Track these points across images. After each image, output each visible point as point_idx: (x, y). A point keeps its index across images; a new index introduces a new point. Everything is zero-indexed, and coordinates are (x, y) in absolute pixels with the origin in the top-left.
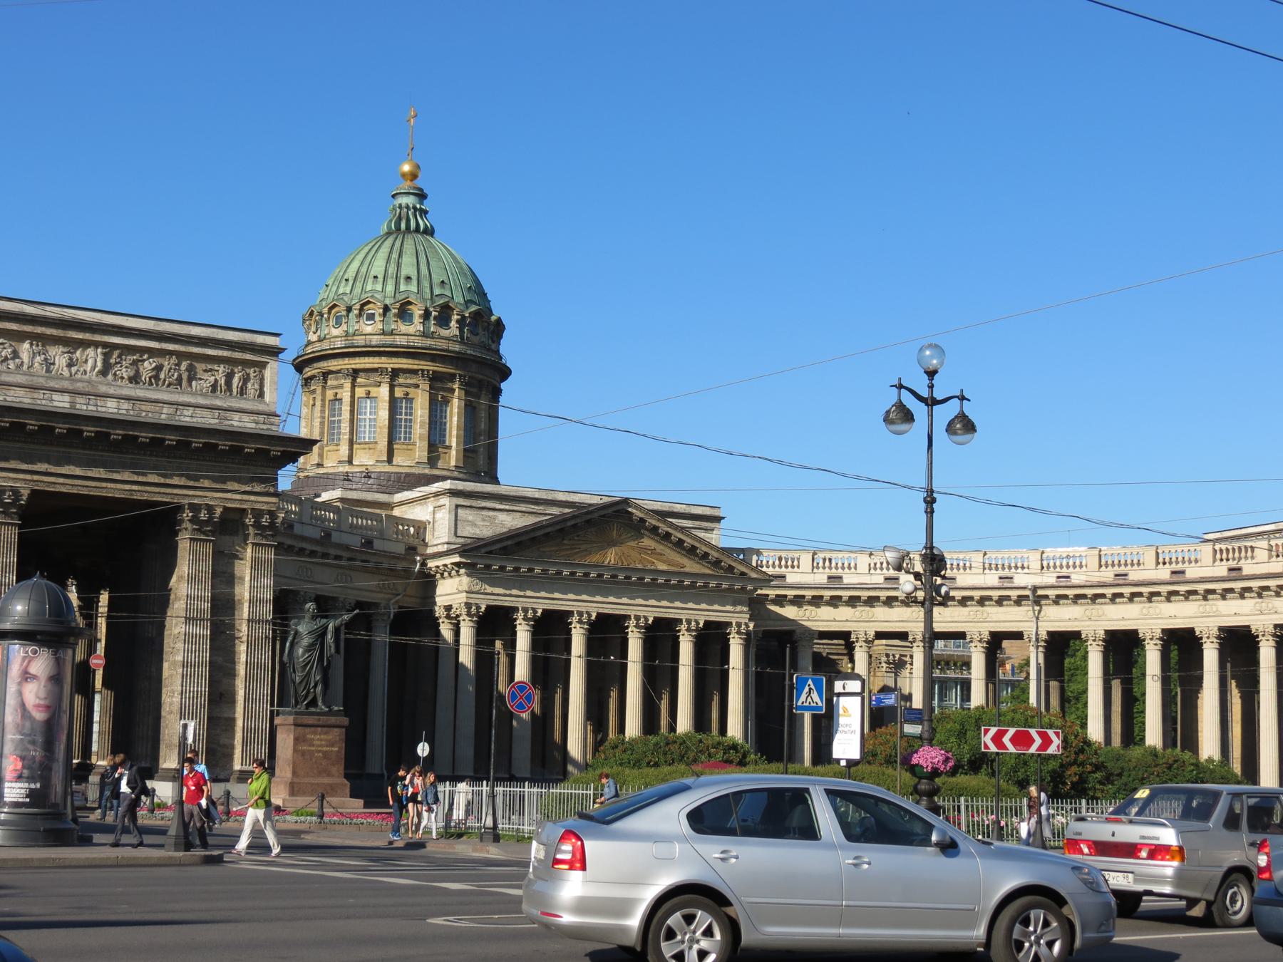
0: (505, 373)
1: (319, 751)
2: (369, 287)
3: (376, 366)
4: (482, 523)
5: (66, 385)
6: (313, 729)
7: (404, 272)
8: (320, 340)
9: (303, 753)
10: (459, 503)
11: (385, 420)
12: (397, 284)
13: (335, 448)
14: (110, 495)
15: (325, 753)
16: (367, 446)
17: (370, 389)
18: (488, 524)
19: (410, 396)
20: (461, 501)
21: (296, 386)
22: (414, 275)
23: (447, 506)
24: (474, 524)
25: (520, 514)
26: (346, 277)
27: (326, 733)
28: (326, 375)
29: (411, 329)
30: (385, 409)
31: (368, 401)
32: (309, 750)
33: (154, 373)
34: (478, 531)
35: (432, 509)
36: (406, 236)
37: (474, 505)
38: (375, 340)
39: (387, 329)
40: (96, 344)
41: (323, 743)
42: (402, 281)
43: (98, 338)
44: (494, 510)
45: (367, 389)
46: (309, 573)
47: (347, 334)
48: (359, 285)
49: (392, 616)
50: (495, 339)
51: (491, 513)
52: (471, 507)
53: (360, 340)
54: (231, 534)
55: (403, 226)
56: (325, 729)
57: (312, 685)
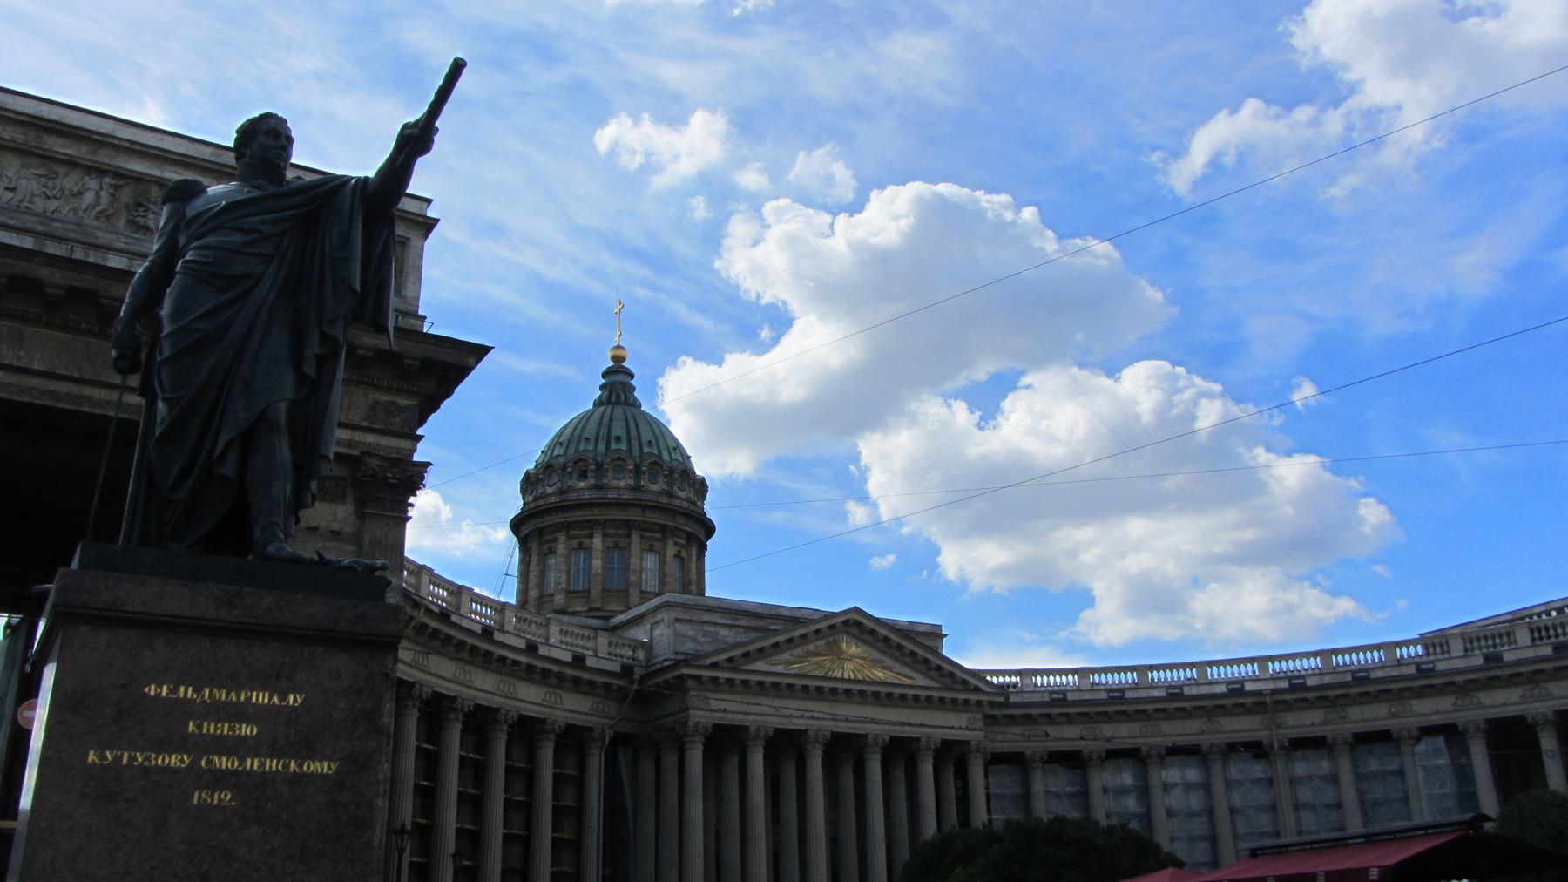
0: (709, 529)
1: (220, 779)
2: (582, 448)
3: (589, 518)
4: (703, 639)
5: (32, 222)
7: (615, 433)
8: (536, 499)
10: (677, 617)
11: (598, 568)
14: (97, 411)
16: (580, 595)
18: (710, 640)
19: (622, 545)
22: (624, 436)
23: (666, 621)
24: (694, 640)
25: (742, 630)
26: (560, 440)
28: (541, 531)
29: (622, 484)
32: (146, 771)
34: (699, 648)
35: (648, 627)
36: (615, 409)
37: (695, 618)
38: (587, 495)
40: (99, 171)
41: (246, 730)
42: (612, 441)
43: (105, 158)
44: (716, 624)
45: (580, 540)
46: (512, 690)
47: (561, 492)
48: (572, 447)
49: (607, 743)
50: (700, 496)
51: (712, 629)
52: (690, 621)
53: (573, 496)
54: (332, 501)
55: (613, 399)
57: (224, 438)
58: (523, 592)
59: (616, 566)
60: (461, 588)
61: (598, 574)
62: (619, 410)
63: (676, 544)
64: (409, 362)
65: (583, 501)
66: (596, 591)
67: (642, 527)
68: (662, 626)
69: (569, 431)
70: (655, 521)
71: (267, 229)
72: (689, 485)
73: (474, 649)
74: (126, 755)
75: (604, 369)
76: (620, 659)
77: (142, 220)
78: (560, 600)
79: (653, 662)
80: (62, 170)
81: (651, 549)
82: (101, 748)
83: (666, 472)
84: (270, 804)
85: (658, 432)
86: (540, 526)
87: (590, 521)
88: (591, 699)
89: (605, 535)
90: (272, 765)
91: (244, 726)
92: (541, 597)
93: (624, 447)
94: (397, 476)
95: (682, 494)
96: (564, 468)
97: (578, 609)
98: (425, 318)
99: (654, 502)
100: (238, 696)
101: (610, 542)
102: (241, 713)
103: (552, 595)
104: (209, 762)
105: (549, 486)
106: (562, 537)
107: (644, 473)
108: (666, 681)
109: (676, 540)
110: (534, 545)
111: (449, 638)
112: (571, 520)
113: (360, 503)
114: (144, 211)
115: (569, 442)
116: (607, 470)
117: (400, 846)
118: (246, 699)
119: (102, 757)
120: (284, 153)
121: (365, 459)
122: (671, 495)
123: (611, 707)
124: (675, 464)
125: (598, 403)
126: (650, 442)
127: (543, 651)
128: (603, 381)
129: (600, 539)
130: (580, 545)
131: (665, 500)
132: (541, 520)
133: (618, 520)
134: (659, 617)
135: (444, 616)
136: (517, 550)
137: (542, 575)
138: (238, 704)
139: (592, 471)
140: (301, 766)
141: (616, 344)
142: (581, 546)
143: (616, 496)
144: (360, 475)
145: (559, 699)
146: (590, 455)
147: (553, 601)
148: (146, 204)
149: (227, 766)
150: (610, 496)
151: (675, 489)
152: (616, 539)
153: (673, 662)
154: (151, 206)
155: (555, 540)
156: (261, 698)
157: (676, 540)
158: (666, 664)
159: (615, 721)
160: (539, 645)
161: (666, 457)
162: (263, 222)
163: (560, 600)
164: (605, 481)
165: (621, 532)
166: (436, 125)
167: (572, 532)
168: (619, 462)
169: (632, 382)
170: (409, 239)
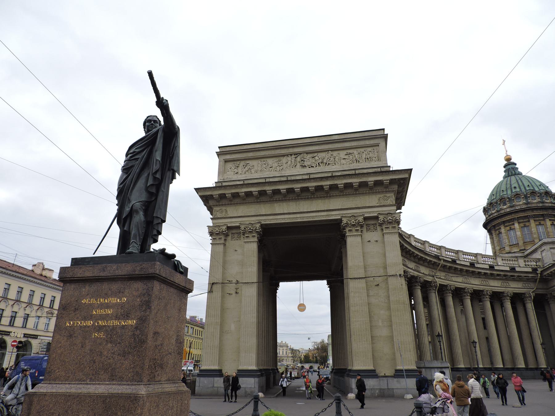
3: (511, 218)
6: (94, 287)
7: (513, 186)
9: (71, 334)
12: (511, 190)
13: (504, 249)
15: (111, 332)
17: (511, 226)
20: (552, 246)
21: (487, 236)
22: (516, 185)
27: (119, 293)
28: (494, 226)
29: (521, 203)
30: (518, 232)
31: (512, 231)
33: (320, 161)
35: (540, 253)
38: (508, 210)
39: (511, 205)
47: (498, 211)
48: (498, 195)
49: (533, 298)
53: (502, 212)
55: (510, 174)
56: (115, 286)
58: (494, 248)
59: (527, 233)
60: (457, 251)
61: (520, 237)
62: (513, 177)
63: (550, 220)
64: (386, 181)
65: (507, 213)
66: (521, 243)
67: (534, 217)
68: (545, 251)
69: (496, 189)
70: (538, 213)
71: (137, 150)
72: (550, 197)
73: (467, 271)
74: (76, 322)
75: (504, 165)
76: (531, 267)
77: (304, 165)
78: (507, 249)
79: (545, 266)
80: (282, 158)
81: (540, 224)
82: (70, 320)
83: (538, 195)
84: (114, 336)
85: (531, 181)
86: (493, 225)
87: (511, 219)
88: (522, 283)
89: (519, 223)
90: (116, 323)
91: (108, 310)
92: (500, 249)
93: (518, 190)
94: (391, 219)
95: (547, 201)
96: (496, 203)
97: (516, 251)
98: (390, 166)
99: (536, 206)
100: (107, 300)
101: (522, 225)
102: (108, 306)
103: (504, 248)
104: (98, 323)
105: (493, 210)
106: (502, 227)
107: (529, 197)
108: (551, 272)
109: (550, 218)
110: (493, 232)
111: (456, 269)
112: (504, 220)
113: (382, 230)
114: (304, 162)
115: (496, 194)
116: (513, 200)
117: (439, 341)
118: (109, 301)
119: (70, 323)
120: (153, 126)
121: (379, 216)
122: (543, 202)
123: (532, 285)
124: (542, 191)
125: (505, 177)
126: (529, 185)
127: (496, 268)
128: (505, 169)
129: (518, 224)
130: (510, 228)
131: (541, 205)
132: (493, 223)
133: (523, 216)
134: (543, 248)
135: (454, 261)
136: (488, 234)
137: (500, 241)
138: (107, 303)
139: (508, 201)
140: (125, 323)
141: (506, 155)
142: (511, 229)
143: (520, 208)
144: (379, 221)
145: (508, 284)
146: (505, 196)
147: (505, 250)
148: (304, 159)
149: (103, 324)
150: (517, 209)
151: (544, 200)
152: (524, 223)
153: (551, 265)
154: (305, 159)
155: (500, 228)
156: (114, 300)
157: (550, 218)
158: (550, 265)
159: (534, 289)
160: (494, 266)
161: (537, 189)
162: (136, 149)
163: (507, 249)
164: (514, 204)
165: (525, 220)
166: (161, 97)
167: (506, 224)
168: (517, 196)
169: (517, 166)
170: (380, 143)
